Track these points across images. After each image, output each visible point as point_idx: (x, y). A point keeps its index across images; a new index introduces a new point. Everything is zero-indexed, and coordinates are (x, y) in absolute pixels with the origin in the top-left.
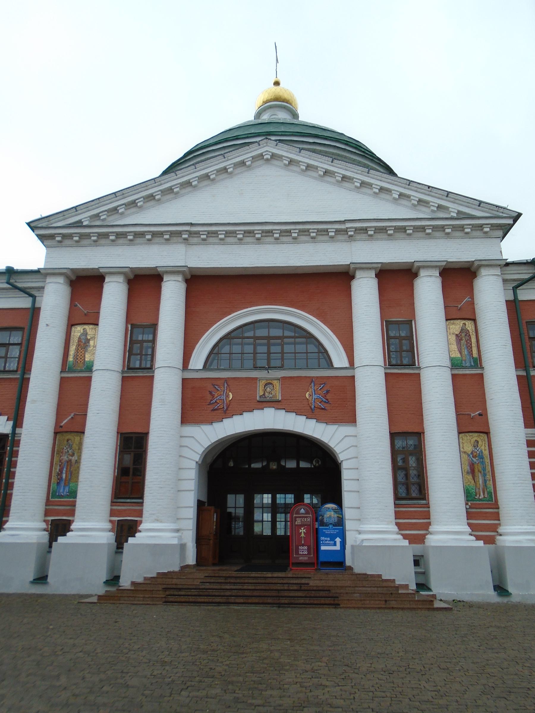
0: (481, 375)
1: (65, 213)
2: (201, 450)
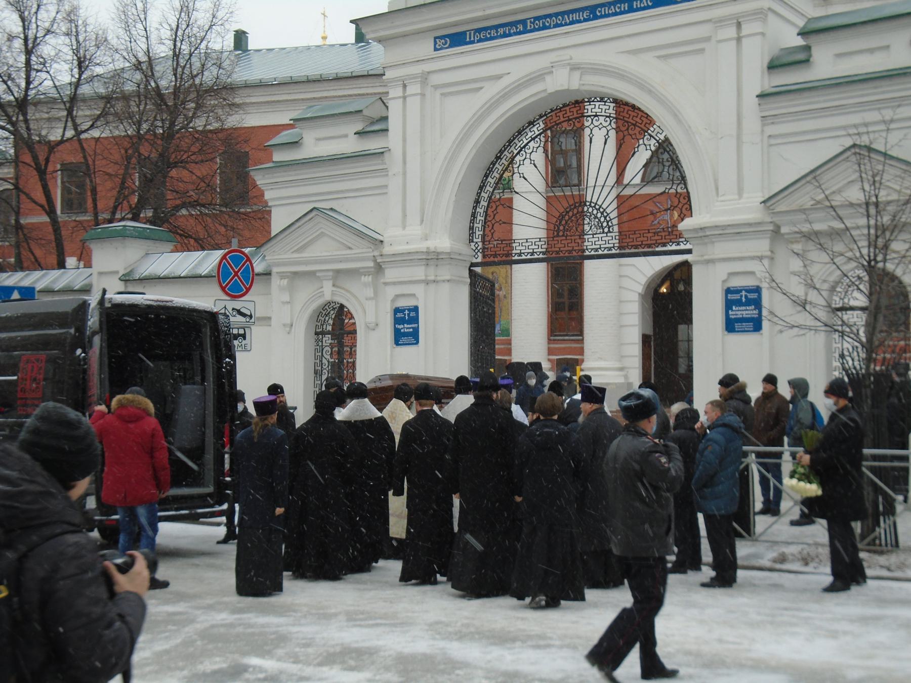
2: (643, 280)
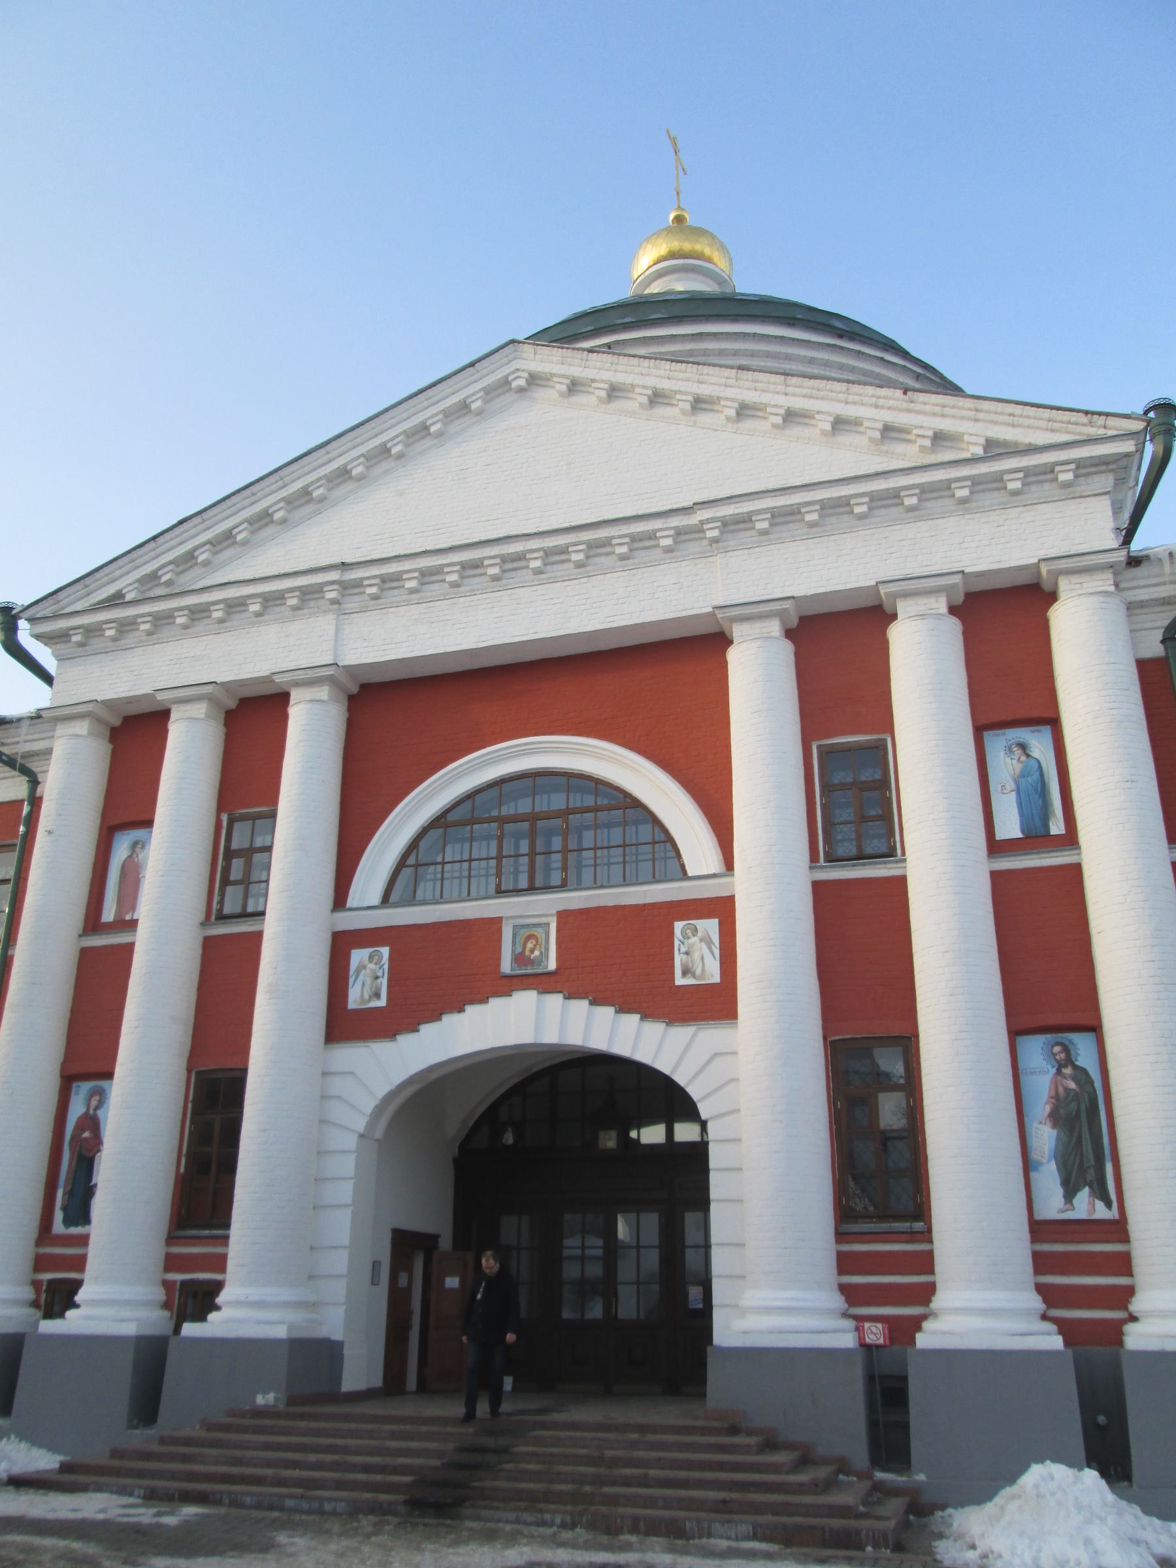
1: (87, 581)
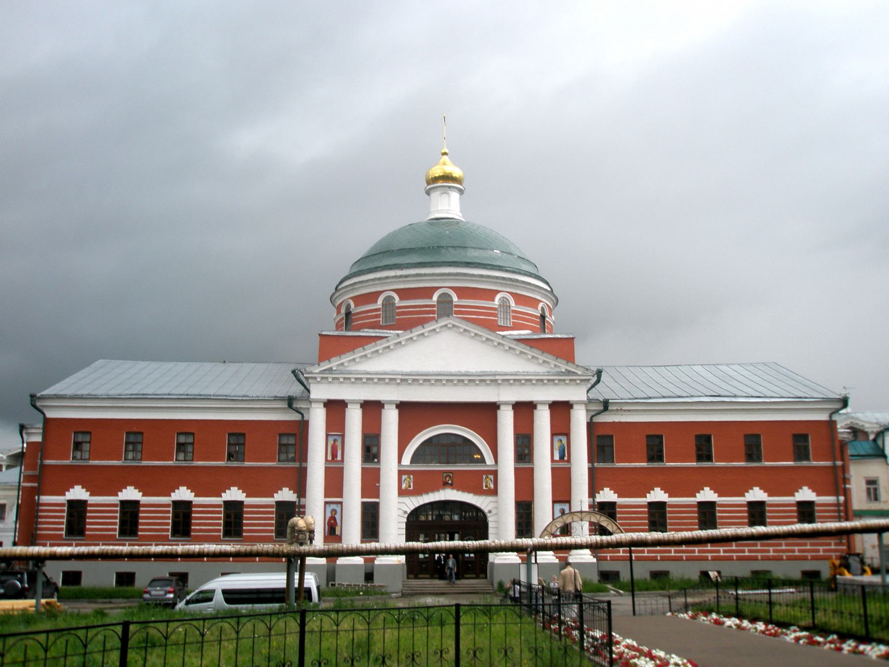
0: (570, 468)
